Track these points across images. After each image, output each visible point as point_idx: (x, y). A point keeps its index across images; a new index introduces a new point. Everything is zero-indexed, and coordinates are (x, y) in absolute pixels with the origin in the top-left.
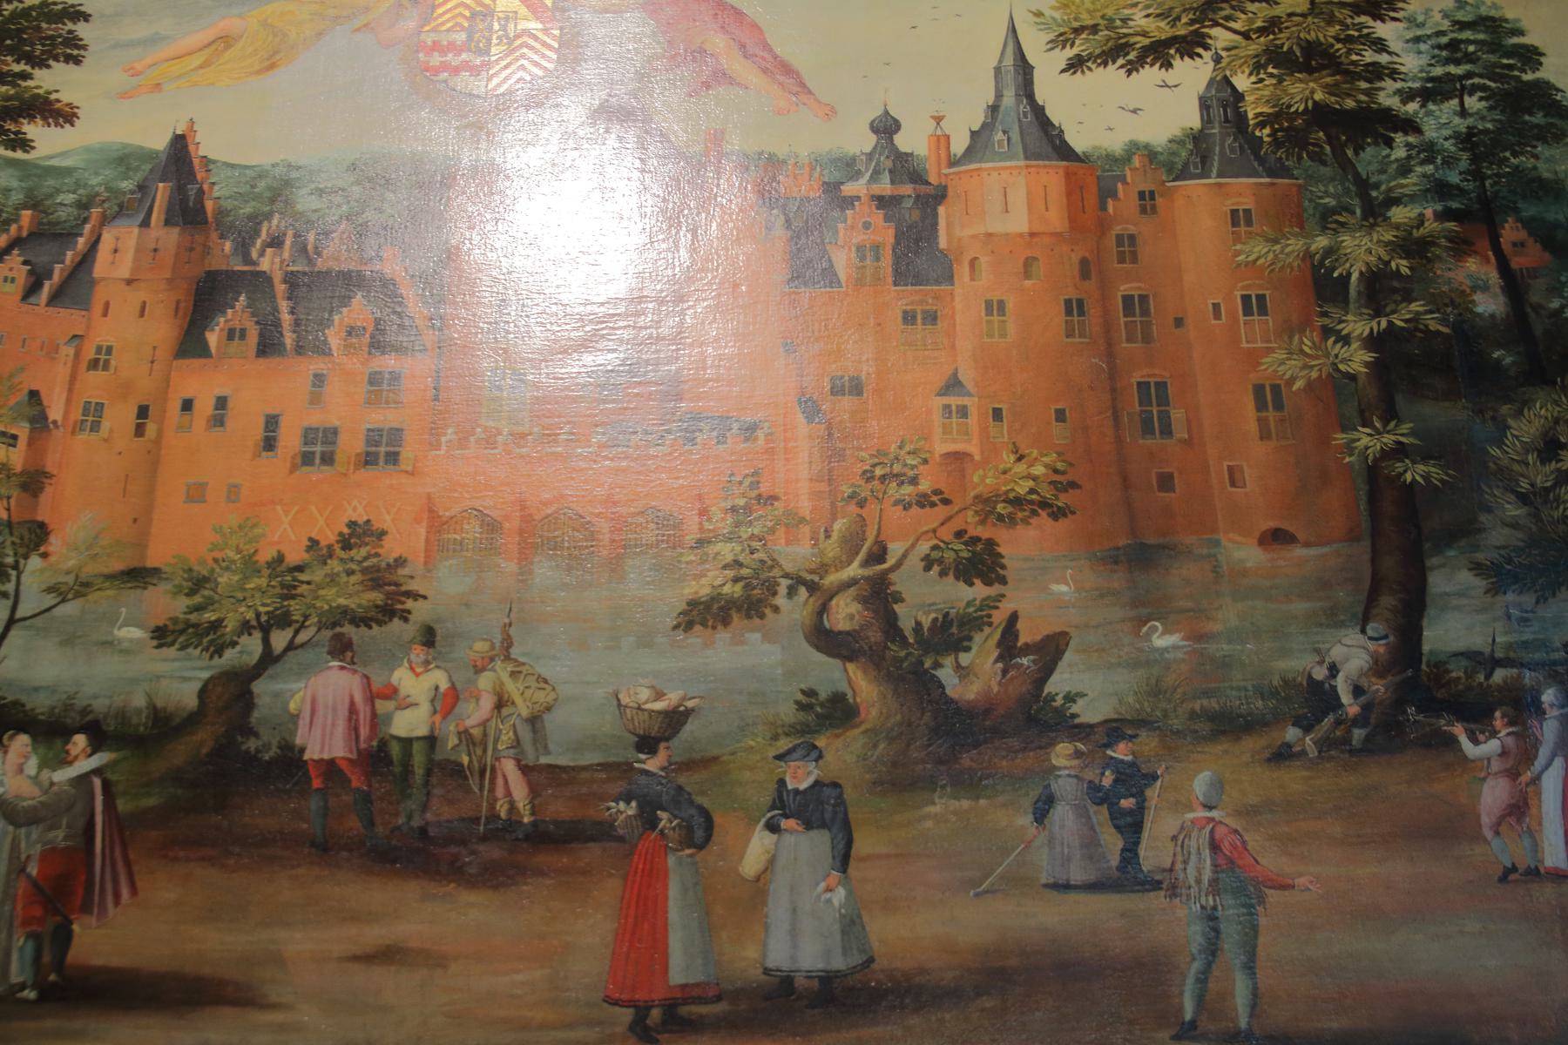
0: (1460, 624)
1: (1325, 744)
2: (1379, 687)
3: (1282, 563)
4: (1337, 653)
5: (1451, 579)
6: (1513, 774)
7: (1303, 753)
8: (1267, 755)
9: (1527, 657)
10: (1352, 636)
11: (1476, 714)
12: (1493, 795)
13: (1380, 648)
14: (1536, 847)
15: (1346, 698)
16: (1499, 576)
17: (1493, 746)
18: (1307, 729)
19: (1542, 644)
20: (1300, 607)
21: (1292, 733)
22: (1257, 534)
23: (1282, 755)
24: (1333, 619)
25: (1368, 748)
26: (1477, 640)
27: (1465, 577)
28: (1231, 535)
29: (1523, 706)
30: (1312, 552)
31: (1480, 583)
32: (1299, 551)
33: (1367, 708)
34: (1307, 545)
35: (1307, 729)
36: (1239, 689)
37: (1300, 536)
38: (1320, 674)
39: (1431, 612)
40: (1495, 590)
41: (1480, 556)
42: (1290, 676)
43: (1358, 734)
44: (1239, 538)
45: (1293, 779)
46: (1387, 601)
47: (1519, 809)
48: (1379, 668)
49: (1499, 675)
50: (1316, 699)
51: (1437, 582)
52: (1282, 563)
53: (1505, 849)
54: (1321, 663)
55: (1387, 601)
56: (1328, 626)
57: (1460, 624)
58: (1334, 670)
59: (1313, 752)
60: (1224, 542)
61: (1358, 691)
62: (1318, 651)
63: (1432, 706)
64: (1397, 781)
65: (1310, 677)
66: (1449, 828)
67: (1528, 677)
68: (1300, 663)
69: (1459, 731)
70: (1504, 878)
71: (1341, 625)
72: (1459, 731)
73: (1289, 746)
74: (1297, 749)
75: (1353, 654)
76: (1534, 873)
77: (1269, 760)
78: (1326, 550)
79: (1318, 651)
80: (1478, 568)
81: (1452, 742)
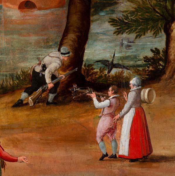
0: (102, 47)
1: (37, 101)
2: (62, 76)
3: (28, 18)
4: (46, 60)
5: (101, 27)
6: (112, 115)
7: (27, 104)
8: (12, 105)
9: (127, 63)
10: (54, 53)
11: (101, 88)
12: (103, 124)
13: (65, 58)
14: (117, 147)
15: (48, 80)
16: (121, 26)
17: (107, 102)
18: (30, 94)
19: (135, 58)
20: (33, 38)
21: (24, 95)
22: (19, 3)
23: (20, 104)
24: (47, 45)
25: (56, 103)
26: (107, 56)
27: (107, 26)
28: (7, 4)
29: (122, 85)
30: (42, 12)
31: (113, 29)
32: (36, 12)
33: (56, 85)
34: (40, 9)
35: (30, 94)
36: (3, 75)
37: (37, 5)
38: (38, 69)
39: (89, 41)
40: (119, 32)
41: (114, 16)
42: (26, 70)
43: (51, 97)
44: (11, 6)
45: (21, 114)
46: (72, 36)
47: (112, 130)
48: (64, 67)
49: (114, 71)
50: (35, 80)
51: (95, 28)
52: (28, 18)
53: (103, 147)
54: (39, 64)
55: (72, 36)
56: (44, 48)
57: (102, 47)
58: (44, 67)
59: (31, 104)
60: (4, 7)
61: (53, 77)
62: (38, 59)
63: (83, 84)
64: (64, 116)
65: (34, 71)
66: (83, 137)
67: (126, 73)
68: (30, 64)
69: (93, 96)
70: (102, 159)
71: (50, 47)
72: (93, 96)
73: (22, 101)
74: (24, 102)
75: (53, 61)
76: (114, 157)
77: (13, 106)
78: (48, 11)
79: (38, 59)
80: (113, 22)
81: (90, 100)
